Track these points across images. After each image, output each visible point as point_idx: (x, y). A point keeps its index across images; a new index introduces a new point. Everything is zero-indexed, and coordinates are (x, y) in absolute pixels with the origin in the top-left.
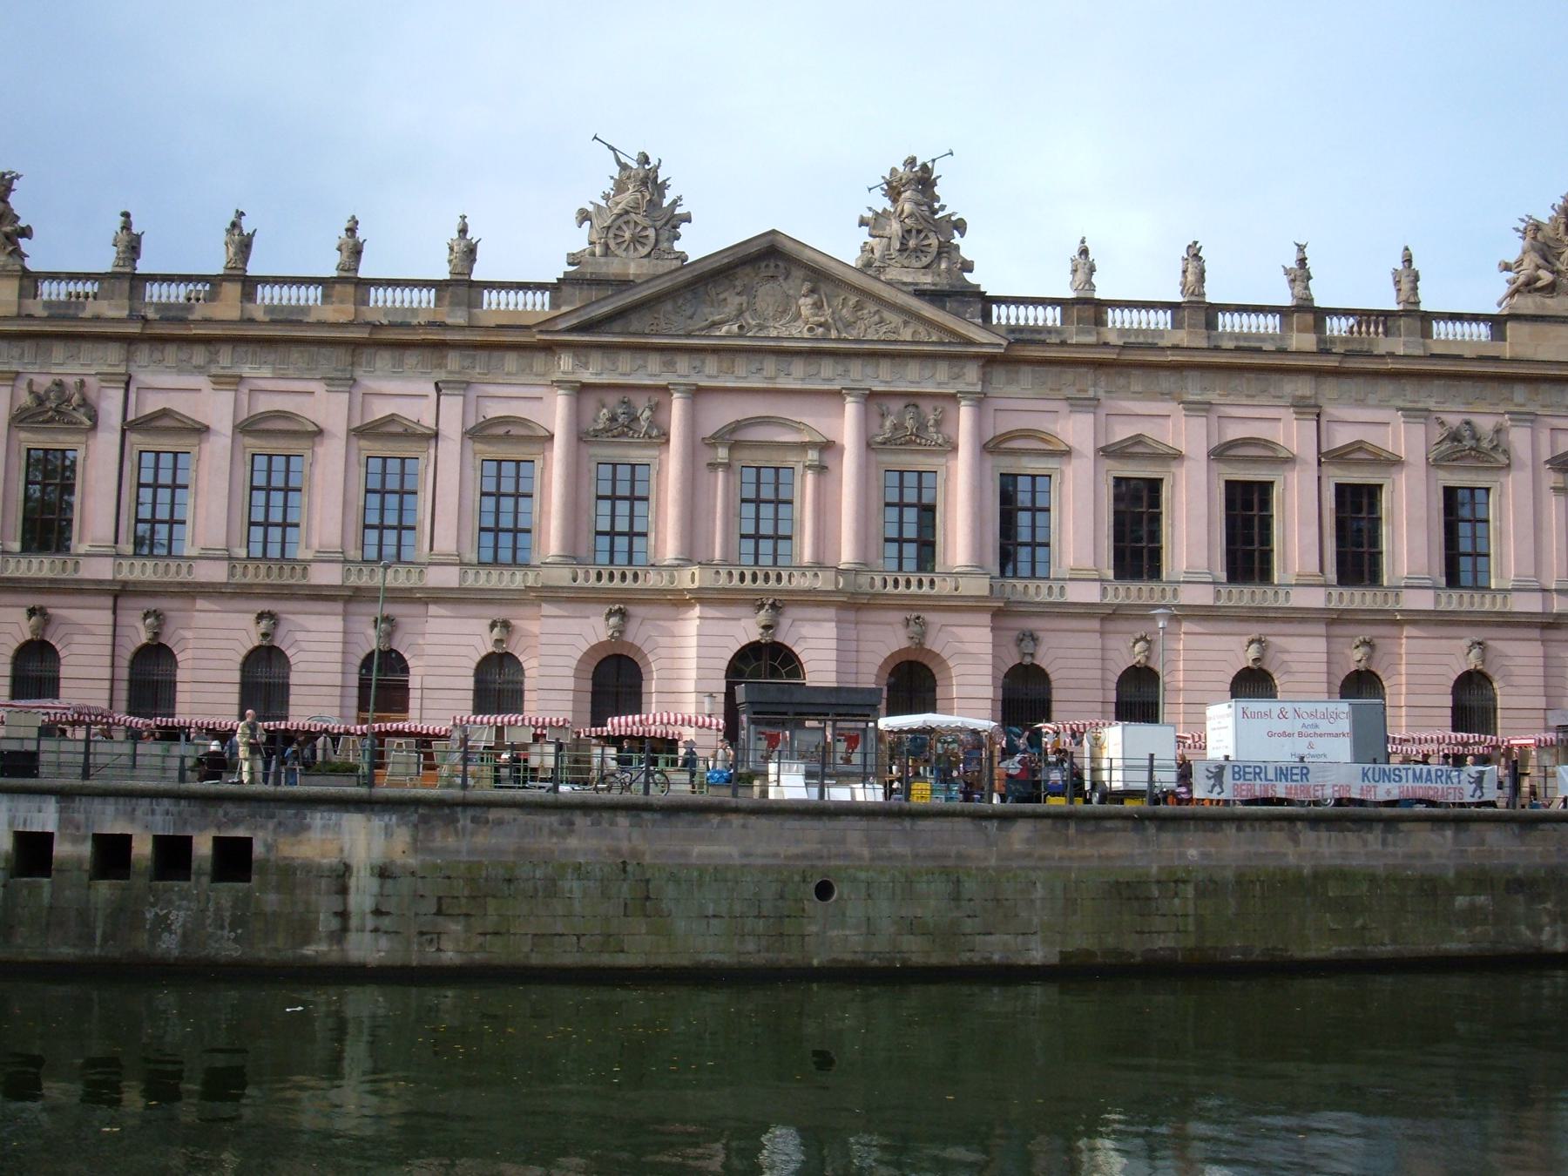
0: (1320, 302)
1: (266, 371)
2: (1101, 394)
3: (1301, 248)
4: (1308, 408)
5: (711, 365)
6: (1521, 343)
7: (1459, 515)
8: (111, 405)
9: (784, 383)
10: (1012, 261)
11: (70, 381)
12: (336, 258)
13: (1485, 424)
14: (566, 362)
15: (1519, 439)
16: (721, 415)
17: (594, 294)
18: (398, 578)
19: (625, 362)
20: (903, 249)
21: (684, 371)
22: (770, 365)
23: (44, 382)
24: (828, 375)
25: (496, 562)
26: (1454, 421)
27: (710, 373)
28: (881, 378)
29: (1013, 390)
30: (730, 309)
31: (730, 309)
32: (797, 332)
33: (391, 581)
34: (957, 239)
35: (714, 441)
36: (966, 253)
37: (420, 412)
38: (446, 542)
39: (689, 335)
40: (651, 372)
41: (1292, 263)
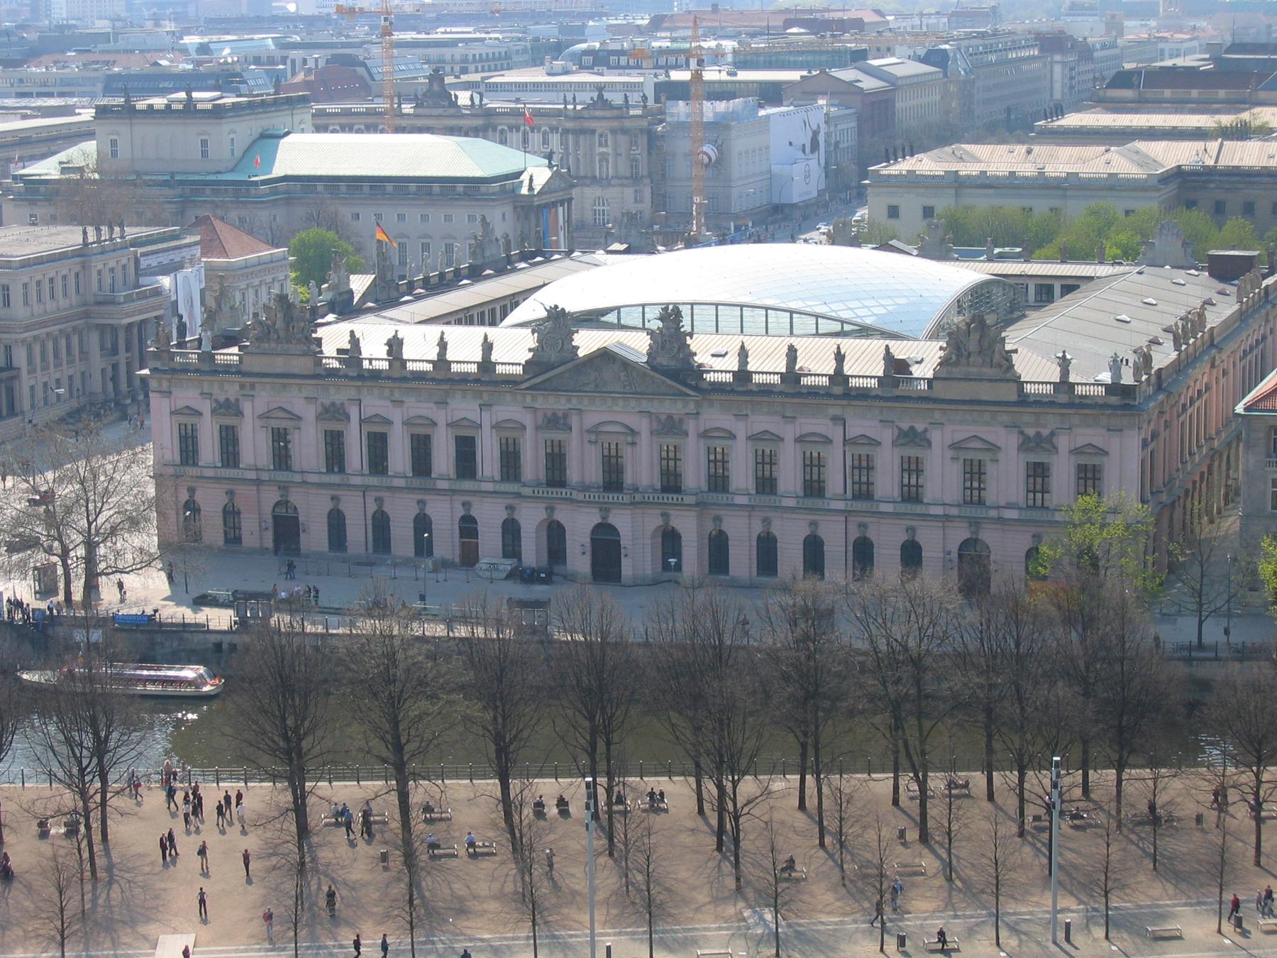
1: (413, 399)
2: (749, 412)
4: (840, 420)
6: (940, 391)
7: (912, 467)
8: (354, 413)
10: (713, 353)
11: (338, 403)
12: (437, 349)
13: (920, 427)
15: (935, 436)
16: (591, 420)
20: (663, 348)
23: (327, 402)
26: (905, 426)
28: (655, 407)
34: (689, 341)
35: (588, 431)
36: (693, 348)
37: (474, 415)
38: (487, 473)
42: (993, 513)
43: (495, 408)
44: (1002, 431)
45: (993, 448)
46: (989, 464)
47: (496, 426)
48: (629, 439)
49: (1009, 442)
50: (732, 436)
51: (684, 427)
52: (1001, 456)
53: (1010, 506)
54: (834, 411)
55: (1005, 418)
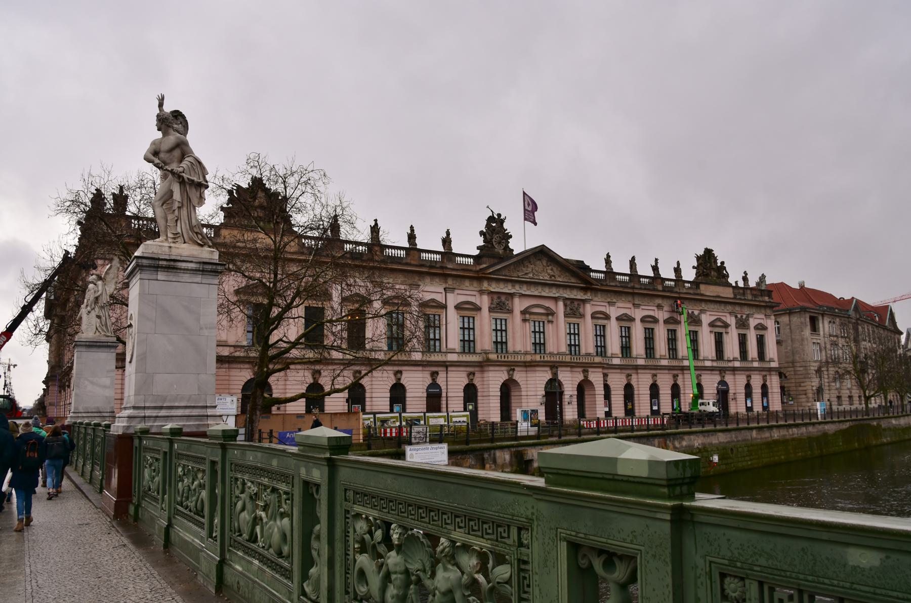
0: (640, 273)
3: (656, 260)
5: (525, 287)
9: (544, 294)
13: (696, 313)
14: (485, 285)
16: (527, 303)
17: (492, 261)
18: (402, 357)
19: (502, 285)
21: (517, 289)
22: (540, 289)
24: (554, 293)
25: (464, 352)
27: (524, 290)
28: (567, 294)
29: (596, 299)
30: (530, 270)
31: (530, 270)
32: (545, 277)
33: (400, 358)
35: (523, 312)
37: (440, 298)
39: (518, 277)
40: (508, 289)
41: (654, 264)
42: (730, 364)
43: (457, 291)
44: (728, 315)
45: (726, 326)
46: (724, 335)
47: (458, 307)
48: (550, 317)
49: (731, 321)
50: (607, 317)
51: (581, 310)
52: (729, 330)
53: (735, 359)
54: (659, 301)
55: (729, 308)
